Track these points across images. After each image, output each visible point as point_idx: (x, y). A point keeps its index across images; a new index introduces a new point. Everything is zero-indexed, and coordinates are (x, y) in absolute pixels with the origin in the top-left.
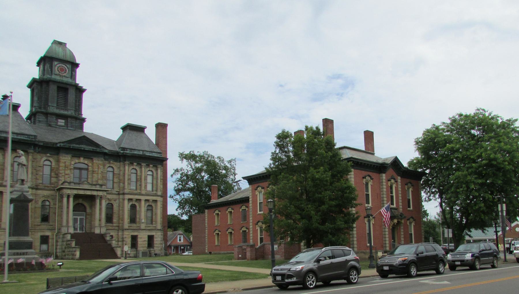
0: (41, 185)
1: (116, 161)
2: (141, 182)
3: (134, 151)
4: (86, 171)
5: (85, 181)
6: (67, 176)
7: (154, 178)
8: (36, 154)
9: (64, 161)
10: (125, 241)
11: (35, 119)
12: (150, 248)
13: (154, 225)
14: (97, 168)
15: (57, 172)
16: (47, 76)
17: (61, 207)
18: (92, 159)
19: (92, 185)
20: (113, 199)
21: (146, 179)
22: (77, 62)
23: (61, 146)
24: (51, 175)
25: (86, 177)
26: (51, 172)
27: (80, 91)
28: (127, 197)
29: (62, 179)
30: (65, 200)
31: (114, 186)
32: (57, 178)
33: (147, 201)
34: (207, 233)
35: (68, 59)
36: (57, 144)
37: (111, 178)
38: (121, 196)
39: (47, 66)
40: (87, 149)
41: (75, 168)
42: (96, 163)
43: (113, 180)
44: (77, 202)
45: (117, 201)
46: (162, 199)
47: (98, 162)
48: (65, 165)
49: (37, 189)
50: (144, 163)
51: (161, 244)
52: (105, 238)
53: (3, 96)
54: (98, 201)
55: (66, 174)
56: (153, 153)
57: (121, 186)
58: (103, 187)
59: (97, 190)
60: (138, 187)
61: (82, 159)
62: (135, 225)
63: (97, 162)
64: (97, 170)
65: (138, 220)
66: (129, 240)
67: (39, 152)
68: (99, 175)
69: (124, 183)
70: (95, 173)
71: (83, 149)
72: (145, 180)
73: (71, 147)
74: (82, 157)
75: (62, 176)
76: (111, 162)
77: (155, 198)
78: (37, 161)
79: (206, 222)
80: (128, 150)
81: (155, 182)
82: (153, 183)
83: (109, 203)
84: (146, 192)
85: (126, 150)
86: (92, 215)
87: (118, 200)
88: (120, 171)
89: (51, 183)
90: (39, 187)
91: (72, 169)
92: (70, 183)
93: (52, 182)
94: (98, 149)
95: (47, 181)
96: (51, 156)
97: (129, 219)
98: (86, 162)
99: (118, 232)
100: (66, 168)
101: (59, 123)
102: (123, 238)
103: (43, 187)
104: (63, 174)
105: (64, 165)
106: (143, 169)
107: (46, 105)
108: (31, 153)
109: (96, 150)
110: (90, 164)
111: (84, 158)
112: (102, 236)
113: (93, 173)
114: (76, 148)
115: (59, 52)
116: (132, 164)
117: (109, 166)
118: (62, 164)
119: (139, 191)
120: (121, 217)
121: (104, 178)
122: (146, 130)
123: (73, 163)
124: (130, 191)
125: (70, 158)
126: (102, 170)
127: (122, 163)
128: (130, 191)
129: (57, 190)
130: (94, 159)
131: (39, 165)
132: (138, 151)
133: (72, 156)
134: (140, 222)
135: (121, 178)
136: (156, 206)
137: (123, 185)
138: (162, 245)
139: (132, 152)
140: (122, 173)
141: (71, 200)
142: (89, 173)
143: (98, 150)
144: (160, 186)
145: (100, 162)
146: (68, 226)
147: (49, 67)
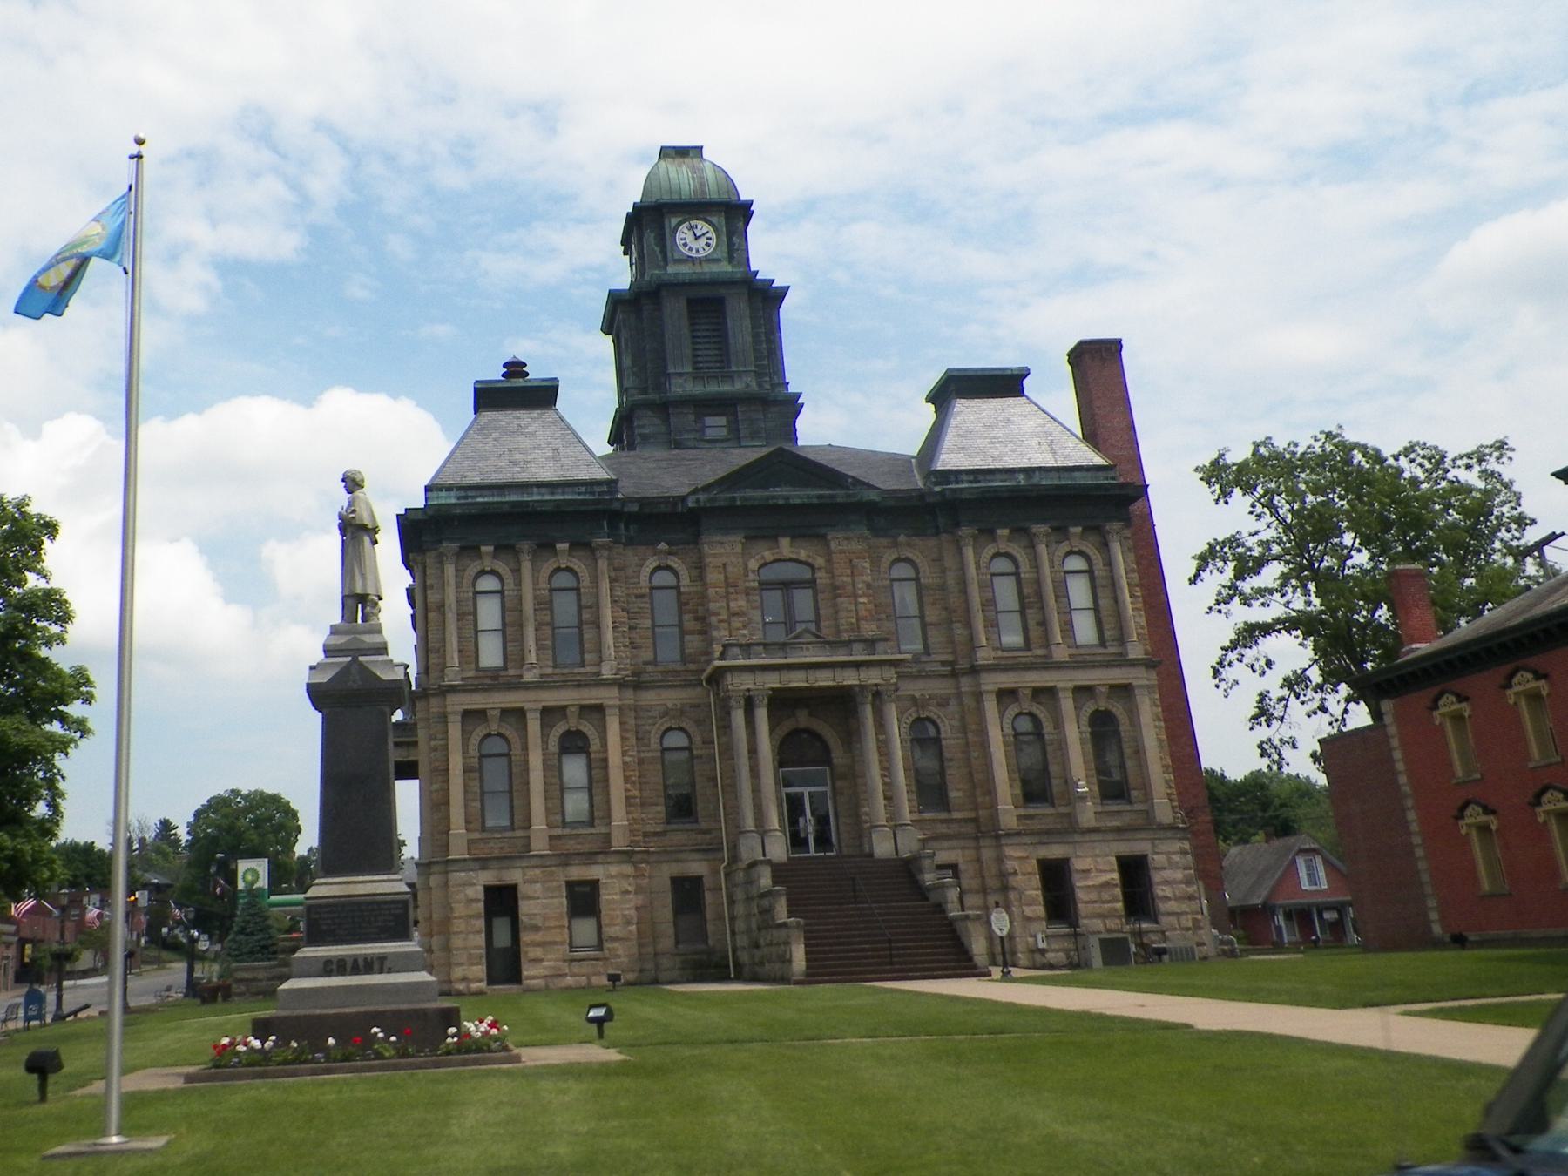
0: (649, 668)
1: (920, 533)
2: (1042, 608)
3: (988, 477)
4: (809, 592)
5: (807, 631)
6: (736, 623)
7: (1098, 582)
8: (619, 549)
9: (718, 561)
10: (1014, 888)
11: (631, 436)
12: (1139, 920)
13: (1138, 807)
14: (849, 572)
15: (700, 608)
16: (653, 273)
17: (728, 752)
18: (824, 537)
19: (834, 645)
20: (931, 698)
21: (1062, 593)
22: (744, 197)
23: (702, 504)
24: (680, 625)
25: (812, 616)
26: (681, 613)
27: (769, 297)
28: (992, 682)
29: (721, 634)
30: (738, 717)
31: (931, 640)
32: (700, 633)
33: (1083, 692)
34: (1414, 827)
35: (713, 195)
36: (683, 499)
37: (913, 609)
38: (966, 683)
39: (650, 237)
40: (798, 501)
41: (765, 585)
42: (842, 552)
43: (922, 617)
44: (787, 726)
45: (953, 707)
46: (1153, 675)
47: (847, 544)
48: (726, 577)
49: (638, 686)
50: (1043, 521)
51: (1191, 898)
52: (919, 877)
53: (504, 366)
54: (868, 712)
55: (734, 615)
56: (1077, 474)
57: (957, 639)
58: (880, 646)
59: (857, 665)
60: (1035, 633)
61: (785, 542)
62: (1050, 810)
63: (844, 546)
64: (849, 579)
65: (1056, 783)
66: (1031, 887)
67: (630, 542)
68: (862, 600)
69: (968, 624)
70: (840, 596)
71: (781, 502)
72: (1057, 597)
73: (738, 503)
74: (784, 536)
75: (721, 621)
76: (902, 538)
77: (1118, 675)
78: (627, 577)
79: (1400, 766)
80: (965, 477)
81: (1105, 603)
82: (1096, 609)
83: (919, 720)
84: (1073, 651)
85: (952, 478)
86: (853, 776)
87: (953, 702)
88: (943, 571)
89: (684, 659)
90: (645, 678)
91: (754, 589)
92: (746, 648)
93: (687, 651)
94: (837, 492)
95: (669, 653)
96: (674, 548)
97: (1018, 784)
98: (802, 555)
99: (978, 848)
100: (732, 590)
101: (710, 433)
102: (1003, 875)
103: (660, 677)
104: (724, 616)
105: (722, 577)
106: (1042, 549)
107: (662, 376)
108: (603, 547)
109: (832, 497)
110: (819, 561)
111: (794, 537)
112: (907, 869)
113: (836, 596)
114: (756, 503)
115: (681, 177)
116: (988, 533)
117: (894, 556)
118: (714, 577)
119: (1040, 652)
120: (978, 777)
121: (885, 610)
122: (1026, 382)
123: (753, 564)
124: (1000, 653)
125: (739, 549)
126: (868, 579)
127: (944, 536)
128: (1000, 653)
129: (709, 681)
130: (829, 537)
131: (635, 592)
132: (1005, 476)
133: (745, 538)
134: (1072, 798)
135: (954, 601)
136: (1133, 713)
137: (966, 632)
138: (1194, 905)
139: (982, 484)
140: (951, 579)
141: (762, 715)
142: (820, 596)
143: (840, 495)
144: (1135, 620)
145: (856, 546)
146: (762, 831)
147: (653, 242)
